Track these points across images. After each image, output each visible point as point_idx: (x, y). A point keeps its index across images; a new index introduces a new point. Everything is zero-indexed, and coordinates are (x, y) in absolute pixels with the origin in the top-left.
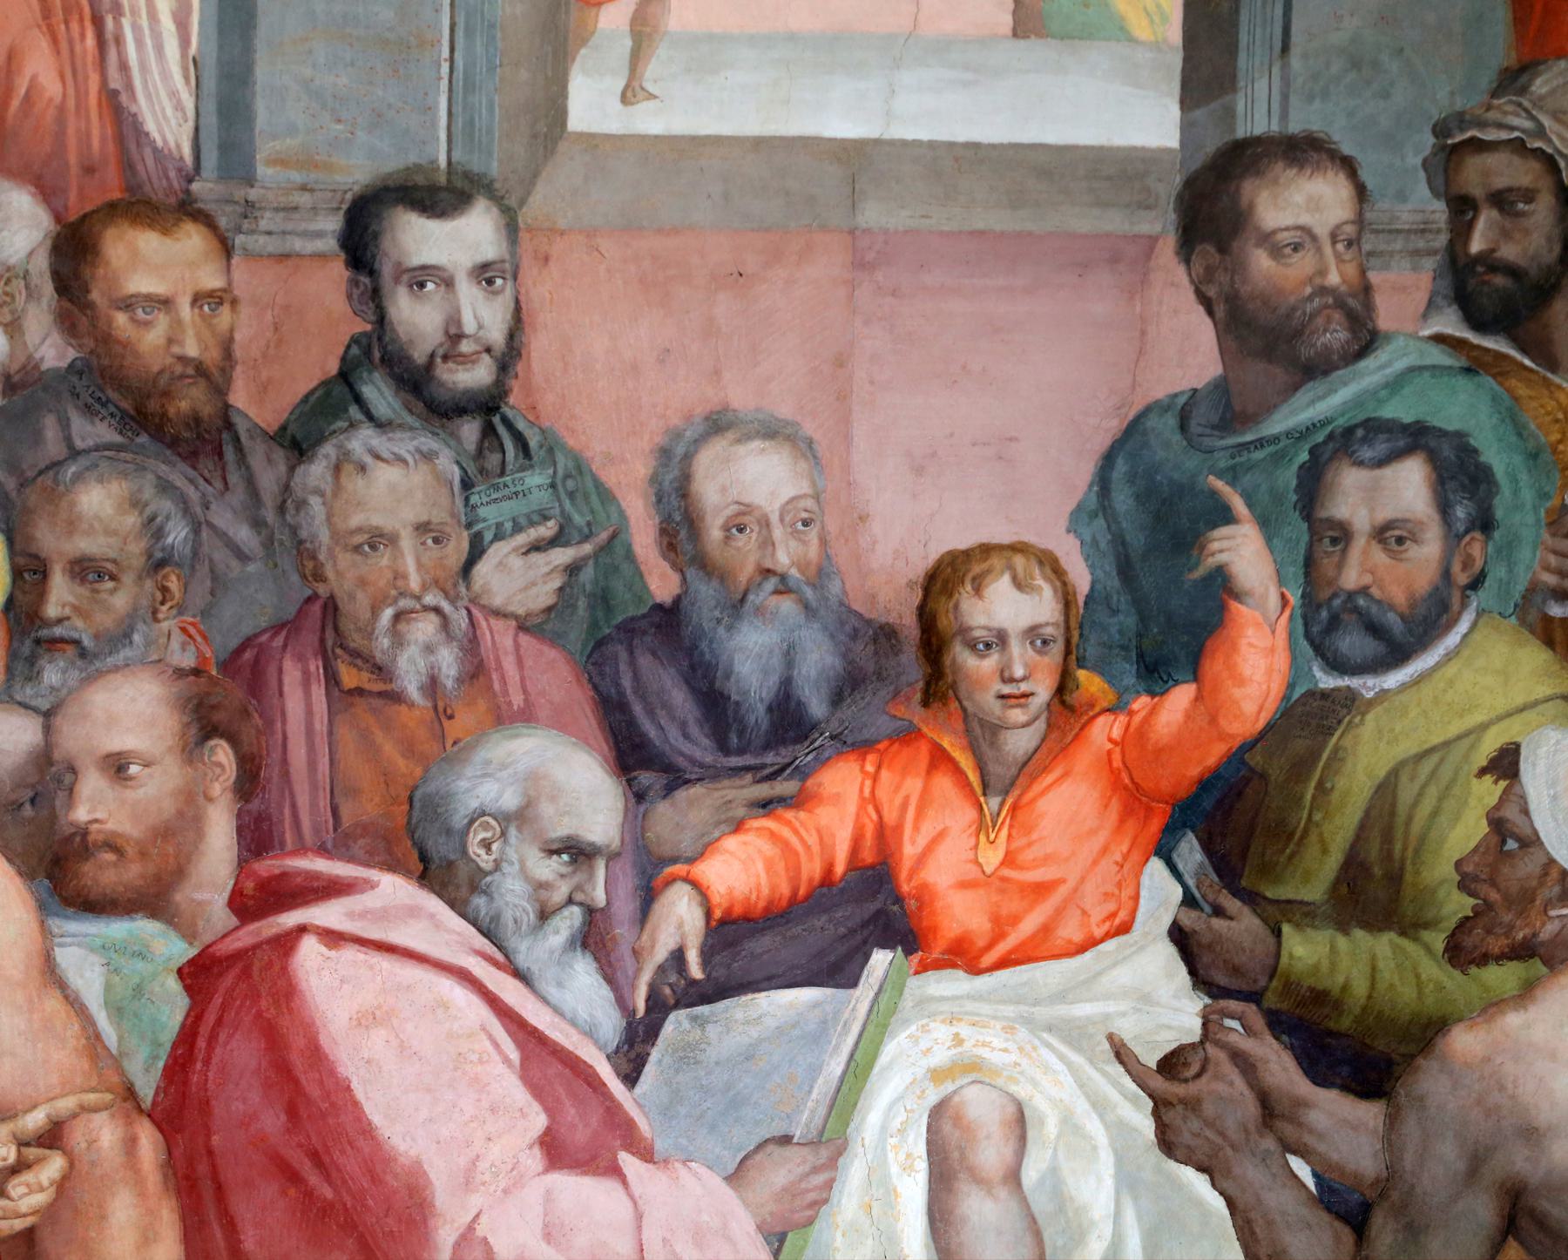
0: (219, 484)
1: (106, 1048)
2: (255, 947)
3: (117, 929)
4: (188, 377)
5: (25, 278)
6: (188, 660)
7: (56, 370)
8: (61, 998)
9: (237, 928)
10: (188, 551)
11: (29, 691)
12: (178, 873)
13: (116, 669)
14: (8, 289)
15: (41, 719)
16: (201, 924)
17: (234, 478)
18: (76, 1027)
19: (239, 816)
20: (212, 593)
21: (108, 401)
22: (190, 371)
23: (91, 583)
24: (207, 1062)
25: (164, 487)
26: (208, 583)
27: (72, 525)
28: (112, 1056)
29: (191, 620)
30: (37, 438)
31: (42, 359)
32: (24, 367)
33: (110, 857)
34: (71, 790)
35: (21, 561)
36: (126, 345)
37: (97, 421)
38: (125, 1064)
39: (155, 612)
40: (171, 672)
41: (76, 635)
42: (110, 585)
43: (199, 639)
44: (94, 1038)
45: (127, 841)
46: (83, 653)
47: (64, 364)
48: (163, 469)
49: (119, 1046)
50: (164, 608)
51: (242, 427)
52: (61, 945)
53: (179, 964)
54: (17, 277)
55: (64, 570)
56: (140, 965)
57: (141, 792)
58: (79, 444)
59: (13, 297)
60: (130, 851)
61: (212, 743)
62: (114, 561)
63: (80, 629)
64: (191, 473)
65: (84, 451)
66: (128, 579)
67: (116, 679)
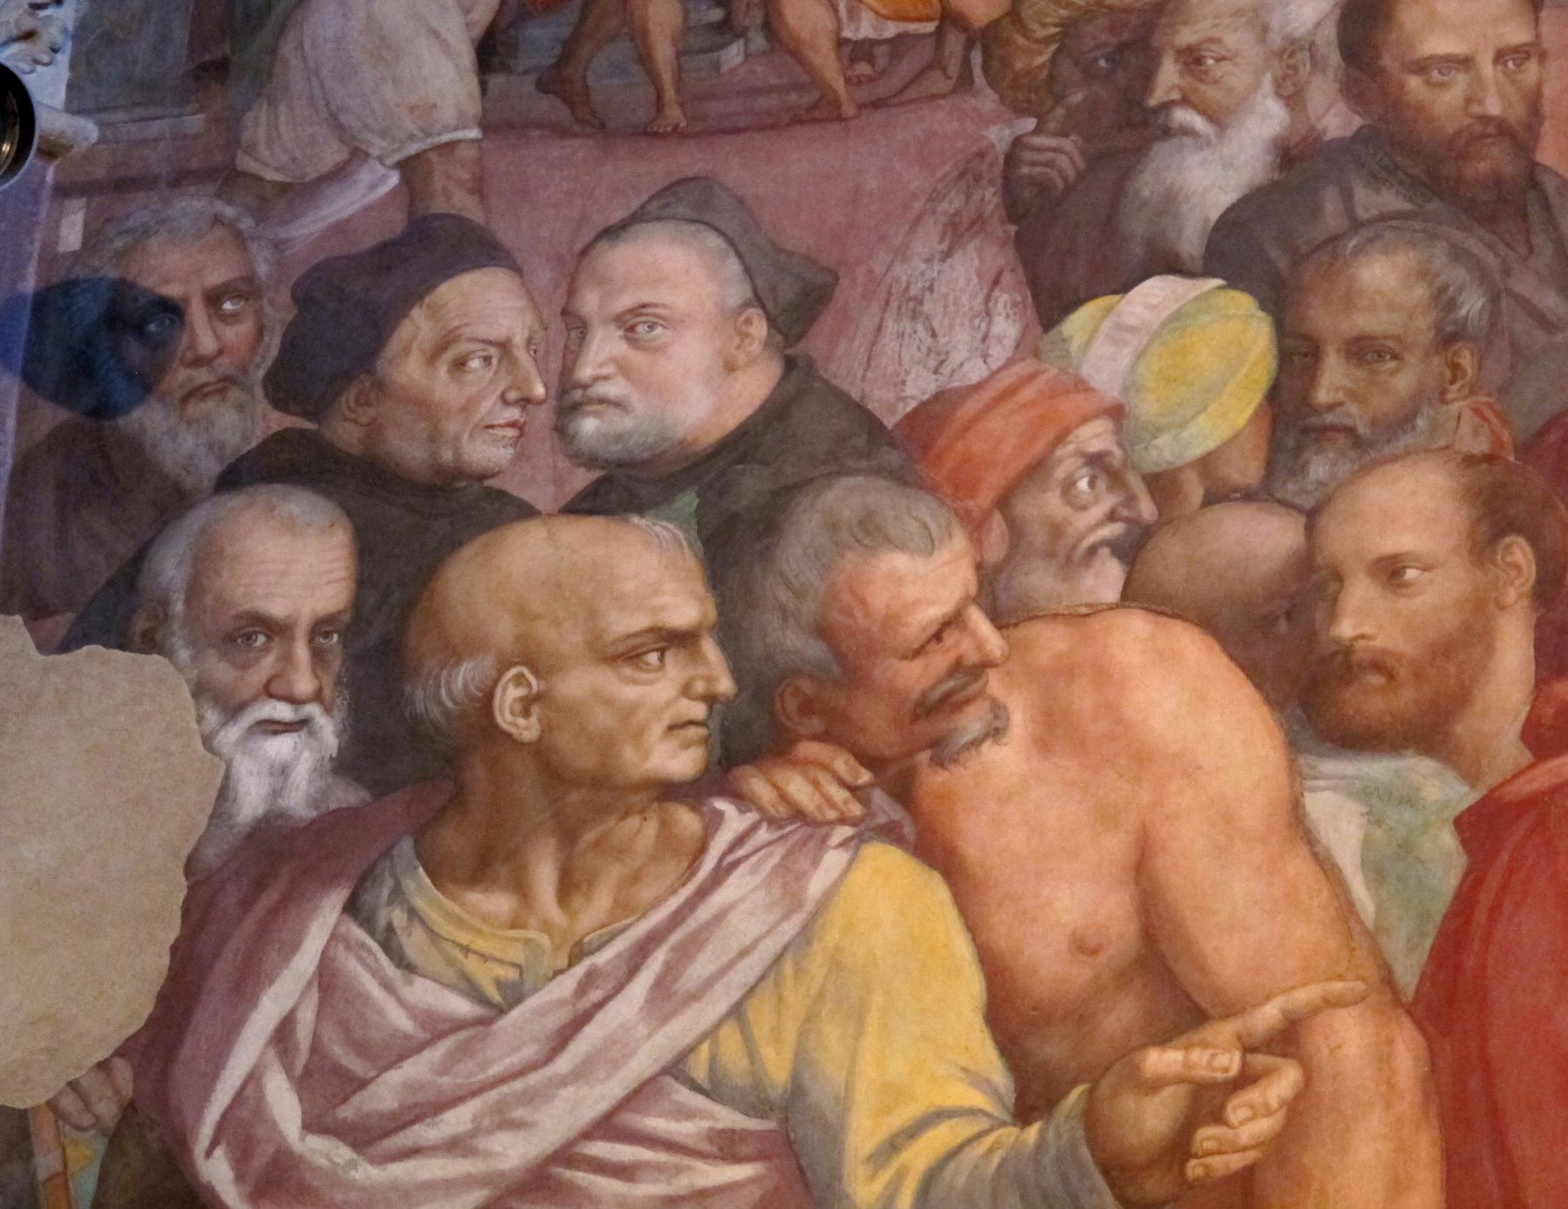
0: (1522, 250)
1: (1362, 923)
2: (1554, 790)
3: (1378, 768)
4: (1489, 136)
5: (1310, 49)
6: (1481, 446)
7: (1338, 142)
8: (1309, 856)
9: (1531, 767)
10: (1484, 322)
11: (1291, 487)
12: (1459, 699)
13: (1395, 458)
14: (1292, 62)
15: (1303, 519)
16: (1485, 761)
17: (1540, 240)
18: (1326, 893)
19: (1538, 627)
20: (1513, 367)
21: (1397, 167)
22: (1491, 130)
23: (1369, 363)
24: (1487, 939)
25: (1458, 254)
26: (1508, 357)
27: (1349, 302)
28: (1366, 932)
29: (1484, 399)
30: (1316, 211)
31: (1324, 131)
32: (1304, 139)
33: (1376, 680)
34: (1335, 600)
35: (1289, 342)
36: (1420, 108)
37: (1384, 190)
38: (1383, 940)
39: (1443, 393)
40: (1459, 460)
41: (1348, 422)
42: (1392, 365)
43: (1495, 421)
44: (1347, 908)
45: (1399, 660)
46: (1358, 443)
47: (1349, 133)
48: (1458, 236)
49: (1377, 920)
50: (1455, 387)
51: (1550, 185)
52: (1313, 790)
53: (1456, 813)
54: (1301, 49)
55: (1338, 351)
56: (1408, 815)
57: (1418, 602)
58: (1362, 214)
59: (1296, 69)
60: (1403, 673)
61: (1508, 540)
62: (1397, 339)
63: (1354, 414)
64: (1494, 238)
65: (1368, 221)
66: (1412, 359)
67: (1395, 469)
